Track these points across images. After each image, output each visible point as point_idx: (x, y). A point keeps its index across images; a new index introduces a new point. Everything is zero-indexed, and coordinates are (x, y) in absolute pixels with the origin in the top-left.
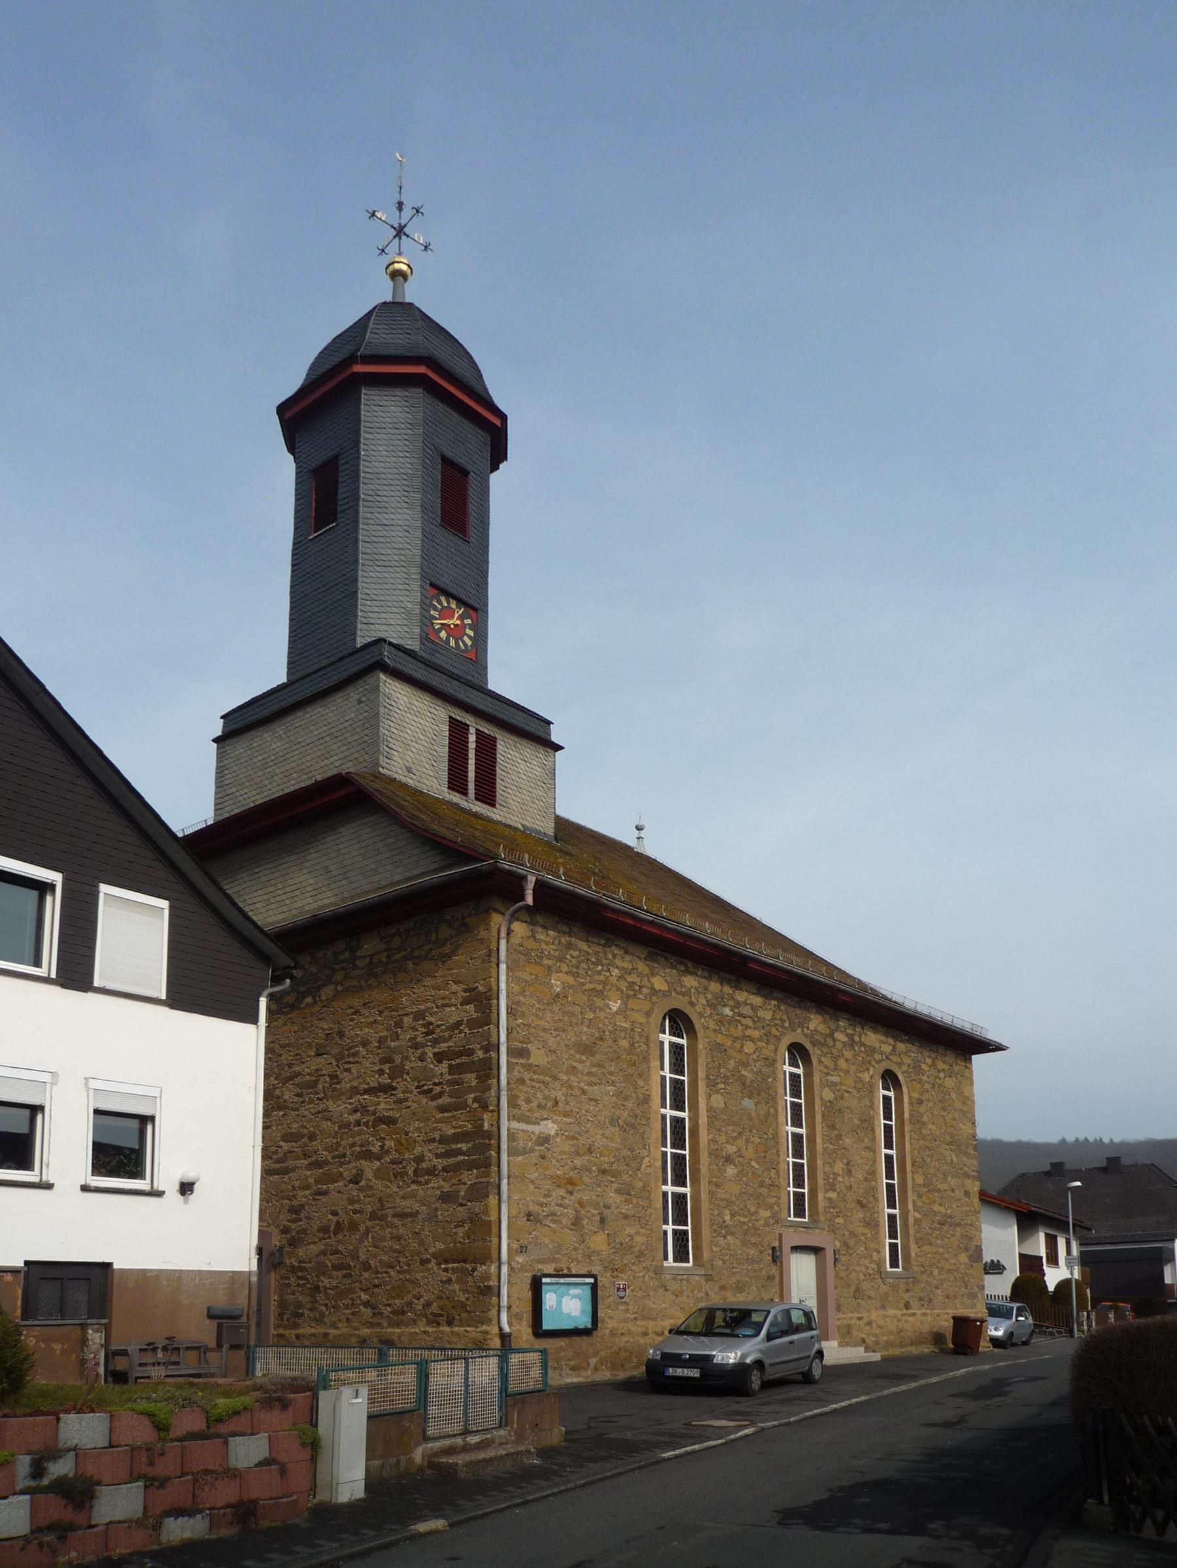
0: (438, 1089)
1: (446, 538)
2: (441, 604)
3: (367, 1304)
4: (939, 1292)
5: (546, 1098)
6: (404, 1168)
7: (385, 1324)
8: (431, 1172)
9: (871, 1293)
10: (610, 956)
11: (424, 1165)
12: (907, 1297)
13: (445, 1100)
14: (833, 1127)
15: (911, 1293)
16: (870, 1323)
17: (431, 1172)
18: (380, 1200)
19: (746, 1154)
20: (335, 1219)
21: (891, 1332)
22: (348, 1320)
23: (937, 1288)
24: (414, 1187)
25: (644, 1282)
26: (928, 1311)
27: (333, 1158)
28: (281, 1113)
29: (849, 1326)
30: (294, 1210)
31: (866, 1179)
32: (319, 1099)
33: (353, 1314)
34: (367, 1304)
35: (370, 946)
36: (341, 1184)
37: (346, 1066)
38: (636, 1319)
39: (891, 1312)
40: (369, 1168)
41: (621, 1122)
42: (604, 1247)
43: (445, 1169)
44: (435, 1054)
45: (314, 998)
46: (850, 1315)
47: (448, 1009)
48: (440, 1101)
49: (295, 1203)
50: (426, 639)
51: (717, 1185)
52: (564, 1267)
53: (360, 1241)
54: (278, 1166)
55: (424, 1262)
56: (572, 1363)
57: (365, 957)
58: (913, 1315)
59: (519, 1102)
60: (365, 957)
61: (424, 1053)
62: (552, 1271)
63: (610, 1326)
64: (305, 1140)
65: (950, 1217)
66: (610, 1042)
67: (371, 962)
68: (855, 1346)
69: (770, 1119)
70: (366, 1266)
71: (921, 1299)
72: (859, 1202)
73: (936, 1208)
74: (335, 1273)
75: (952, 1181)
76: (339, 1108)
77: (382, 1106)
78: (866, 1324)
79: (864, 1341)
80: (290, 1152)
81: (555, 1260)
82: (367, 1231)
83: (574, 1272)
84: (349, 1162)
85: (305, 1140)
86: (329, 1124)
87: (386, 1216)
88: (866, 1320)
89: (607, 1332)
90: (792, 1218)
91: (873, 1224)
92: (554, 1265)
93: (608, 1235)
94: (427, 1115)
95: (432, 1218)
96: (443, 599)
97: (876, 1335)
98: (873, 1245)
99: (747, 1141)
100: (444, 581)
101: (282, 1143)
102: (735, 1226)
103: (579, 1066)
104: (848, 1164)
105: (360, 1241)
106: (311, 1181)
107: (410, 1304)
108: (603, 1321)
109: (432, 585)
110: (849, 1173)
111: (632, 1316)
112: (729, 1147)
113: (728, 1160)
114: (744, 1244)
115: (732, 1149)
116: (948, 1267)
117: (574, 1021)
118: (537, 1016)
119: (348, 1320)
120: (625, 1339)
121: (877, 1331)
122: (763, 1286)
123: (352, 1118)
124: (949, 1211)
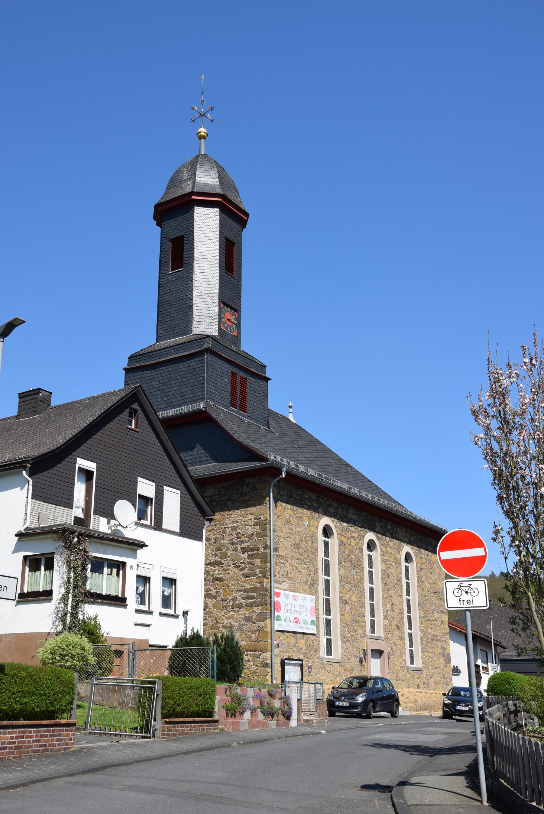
0: (243, 566)
4: (432, 680)
9: (403, 678)
12: (418, 681)
15: (420, 679)
21: (411, 702)
23: (431, 678)
26: (427, 691)
31: (400, 613)
39: (412, 690)
44: (241, 548)
48: (244, 572)
58: (421, 692)
65: (436, 636)
69: (361, 581)
71: (424, 684)
72: (397, 626)
73: (430, 630)
75: (436, 615)
91: (402, 638)
98: (403, 651)
104: (392, 605)
110: (393, 609)
116: (435, 665)
121: (406, 700)
124: (435, 633)
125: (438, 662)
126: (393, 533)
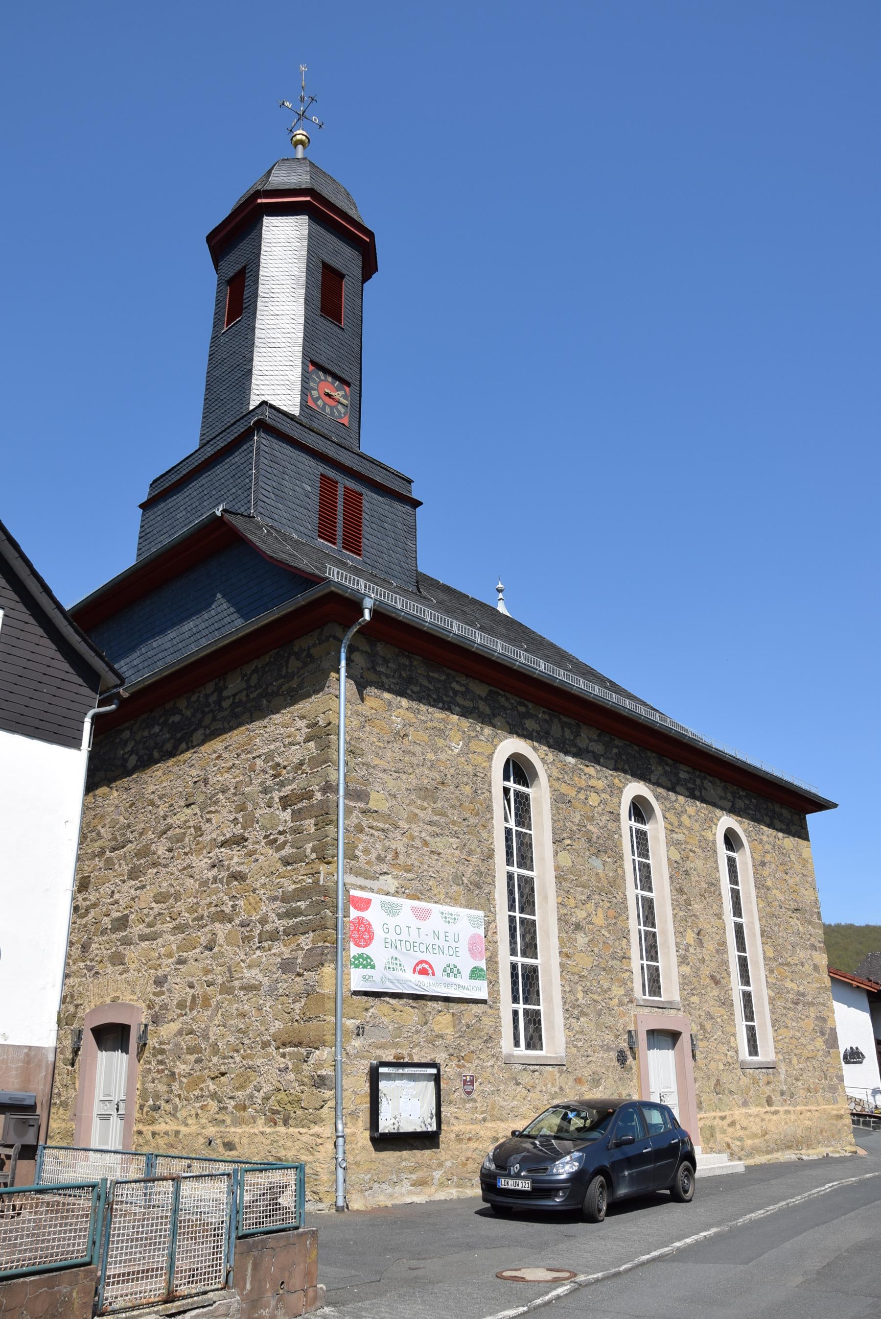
0: (282, 838)
1: (325, 325)
2: (319, 377)
3: (214, 1096)
4: (800, 1084)
5: (387, 849)
6: (251, 930)
7: (229, 1122)
8: (274, 936)
9: (733, 1087)
10: (451, 694)
11: (268, 927)
12: (768, 1090)
13: (288, 851)
14: (681, 891)
15: (772, 1086)
16: (732, 1124)
17: (274, 936)
18: (229, 970)
19: (595, 919)
20: (191, 991)
21: (754, 1136)
22: (197, 1115)
23: (797, 1080)
24: (258, 953)
25: (492, 1074)
26: (791, 1108)
27: (193, 920)
28: (155, 871)
29: (712, 1128)
30: (159, 982)
31: (718, 951)
32: (186, 854)
33: (202, 1108)
34: (214, 1096)
35: (234, 685)
36: (198, 950)
37: (208, 816)
38: (484, 1120)
39: (754, 1110)
40: (221, 929)
41: (466, 881)
42: (450, 1031)
43: (286, 933)
45: (187, 743)
46: (714, 1114)
47: (294, 747)
48: (283, 853)
49: (160, 973)
50: (304, 405)
51: (567, 956)
52: (405, 1052)
53: (211, 1018)
54: (148, 930)
55: (265, 1045)
56: (414, 1177)
57: (229, 698)
58: (776, 1113)
59: (357, 853)
60: (229, 698)
61: (272, 798)
62: (390, 1059)
63: (456, 1128)
64: (172, 900)
66: (452, 788)
67: (233, 703)
68: (720, 1152)
69: (617, 882)
70: (215, 1050)
71: (782, 1093)
72: (712, 977)
74: (189, 1057)
76: (201, 863)
77: (236, 860)
78: (729, 1125)
79: (728, 1146)
80: (159, 914)
81: (396, 1045)
82: (219, 1006)
83: (416, 1061)
84: (207, 925)
85: (172, 900)
86: (192, 881)
87: (233, 988)
88: (728, 1120)
89: (453, 1136)
90: (647, 997)
91: (727, 1003)
92: (393, 1052)
93: (453, 1014)
94: (272, 869)
95: (272, 991)
96: (321, 373)
97: (740, 1139)
98: (728, 1029)
99: (597, 905)
100: (322, 360)
101: (154, 905)
102: (588, 1006)
103: (421, 814)
104: (698, 934)
105: (211, 1018)
106: (174, 947)
107: (251, 1097)
108: (448, 1123)
109: (313, 363)
110: (700, 944)
111: (480, 1117)
112: (578, 911)
113: (578, 927)
114: (598, 1026)
115: (581, 914)
116: (806, 1054)
117: (415, 762)
118: (377, 755)
119: (197, 1115)
120: (473, 1145)
121: (741, 1133)
122: (620, 1079)
123: (210, 874)
125: (810, 1047)
126: (694, 789)
